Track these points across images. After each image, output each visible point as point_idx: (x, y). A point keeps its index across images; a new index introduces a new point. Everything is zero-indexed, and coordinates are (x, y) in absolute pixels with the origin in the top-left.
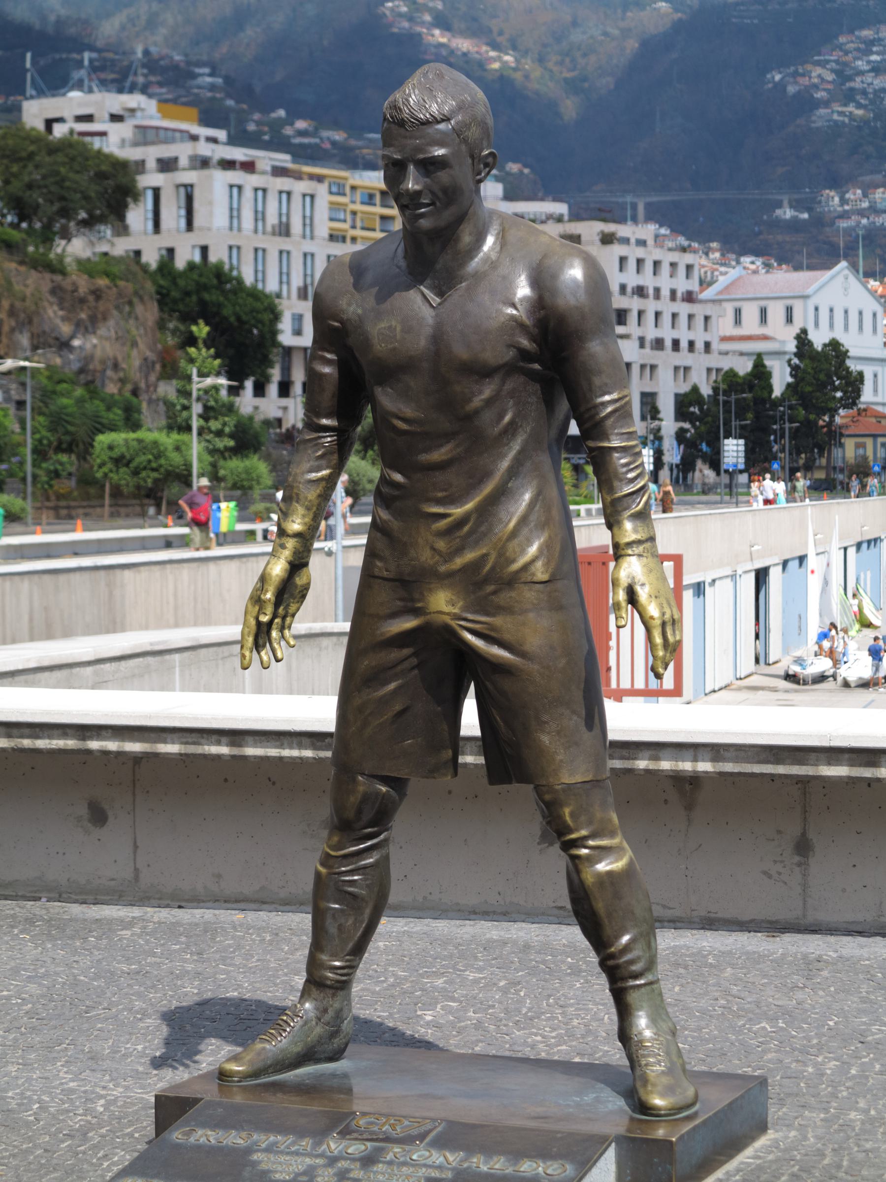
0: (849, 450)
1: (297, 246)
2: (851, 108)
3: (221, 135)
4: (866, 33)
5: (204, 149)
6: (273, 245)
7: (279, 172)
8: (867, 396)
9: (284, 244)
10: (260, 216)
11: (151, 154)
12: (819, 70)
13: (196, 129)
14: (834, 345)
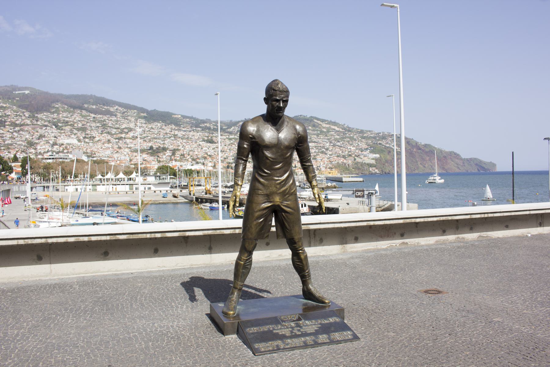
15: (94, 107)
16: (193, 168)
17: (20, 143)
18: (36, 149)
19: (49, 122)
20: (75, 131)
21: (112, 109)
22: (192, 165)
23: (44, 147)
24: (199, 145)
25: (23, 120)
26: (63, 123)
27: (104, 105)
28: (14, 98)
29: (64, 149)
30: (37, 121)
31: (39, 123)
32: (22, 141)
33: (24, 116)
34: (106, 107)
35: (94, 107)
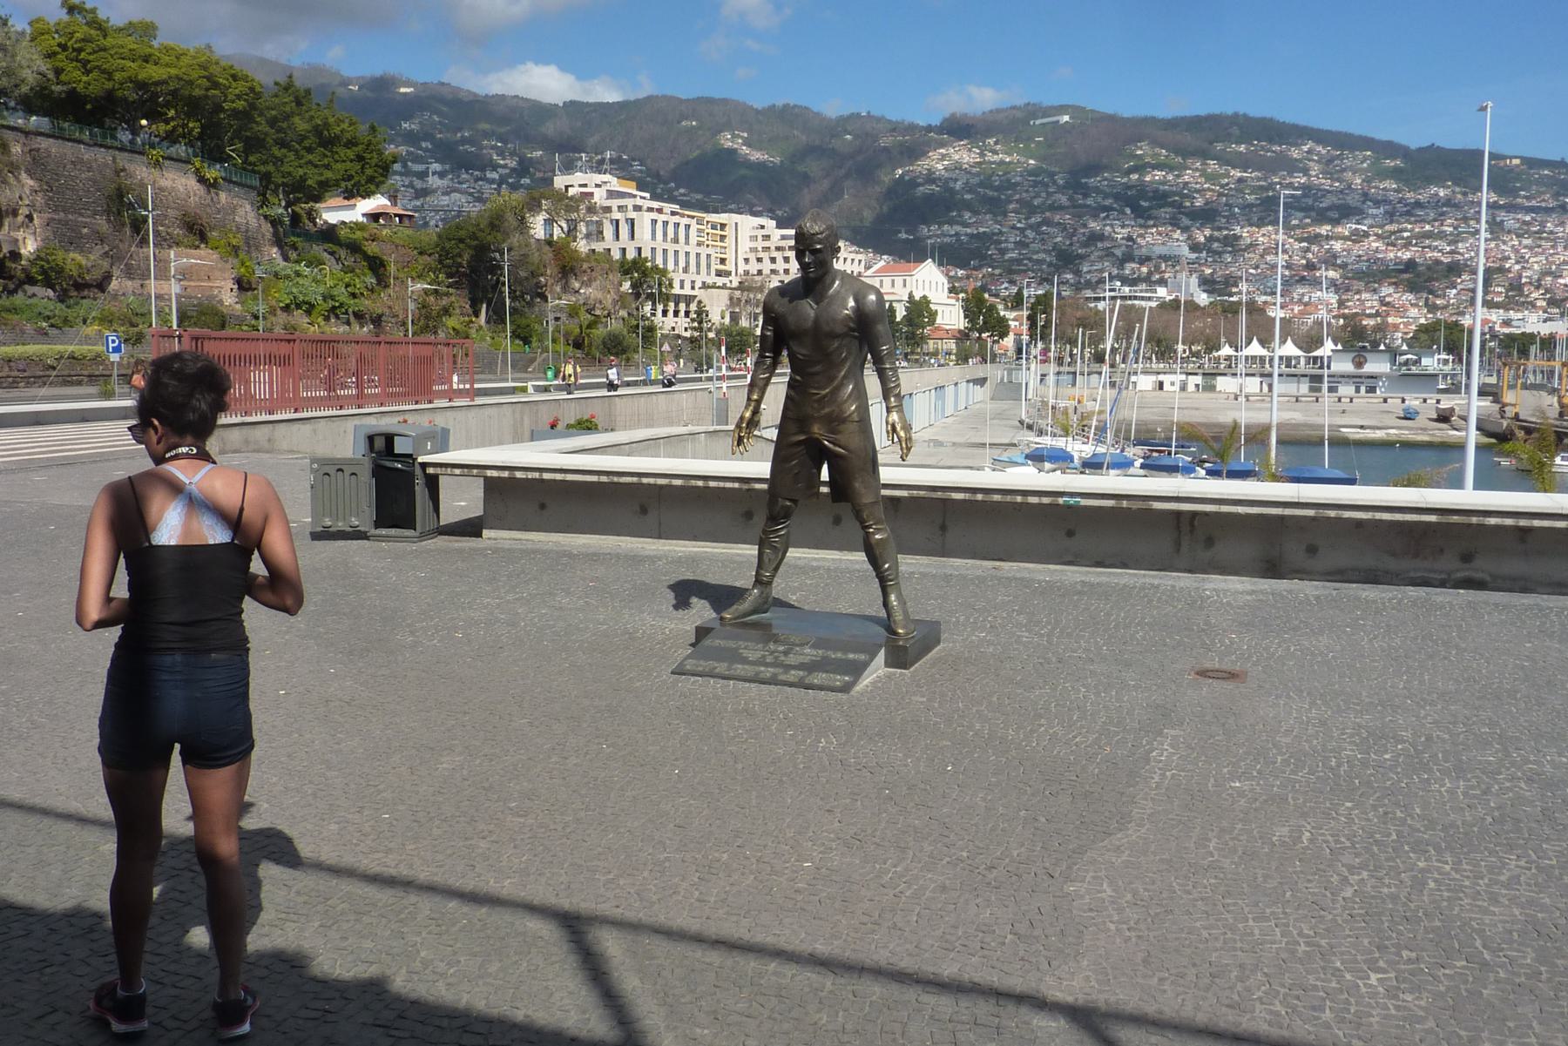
0: (931, 345)
1: (682, 248)
3: (647, 195)
4: (942, 151)
5: (639, 202)
6: (671, 248)
7: (673, 213)
8: (939, 320)
9: (676, 247)
10: (665, 234)
11: (614, 203)
13: (635, 192)
14: (925, 297)
15: (1242, 148)
17: (1041, 256)
18: (1078, 273)
19: (1117, 197)
20: (1185, 221)
21: (1295, 153)
23: (1098, 266)
25: (1049, 194)
26: (1154, 198)
27: (1271, 141)
28: (1030, 139)
29: (1150, 273)
30: (1086, 196)
31: (1089, 201)
32: (1045, 251)
33: (1055, 182)
34: (1276, 148)
35: (1242, 148)
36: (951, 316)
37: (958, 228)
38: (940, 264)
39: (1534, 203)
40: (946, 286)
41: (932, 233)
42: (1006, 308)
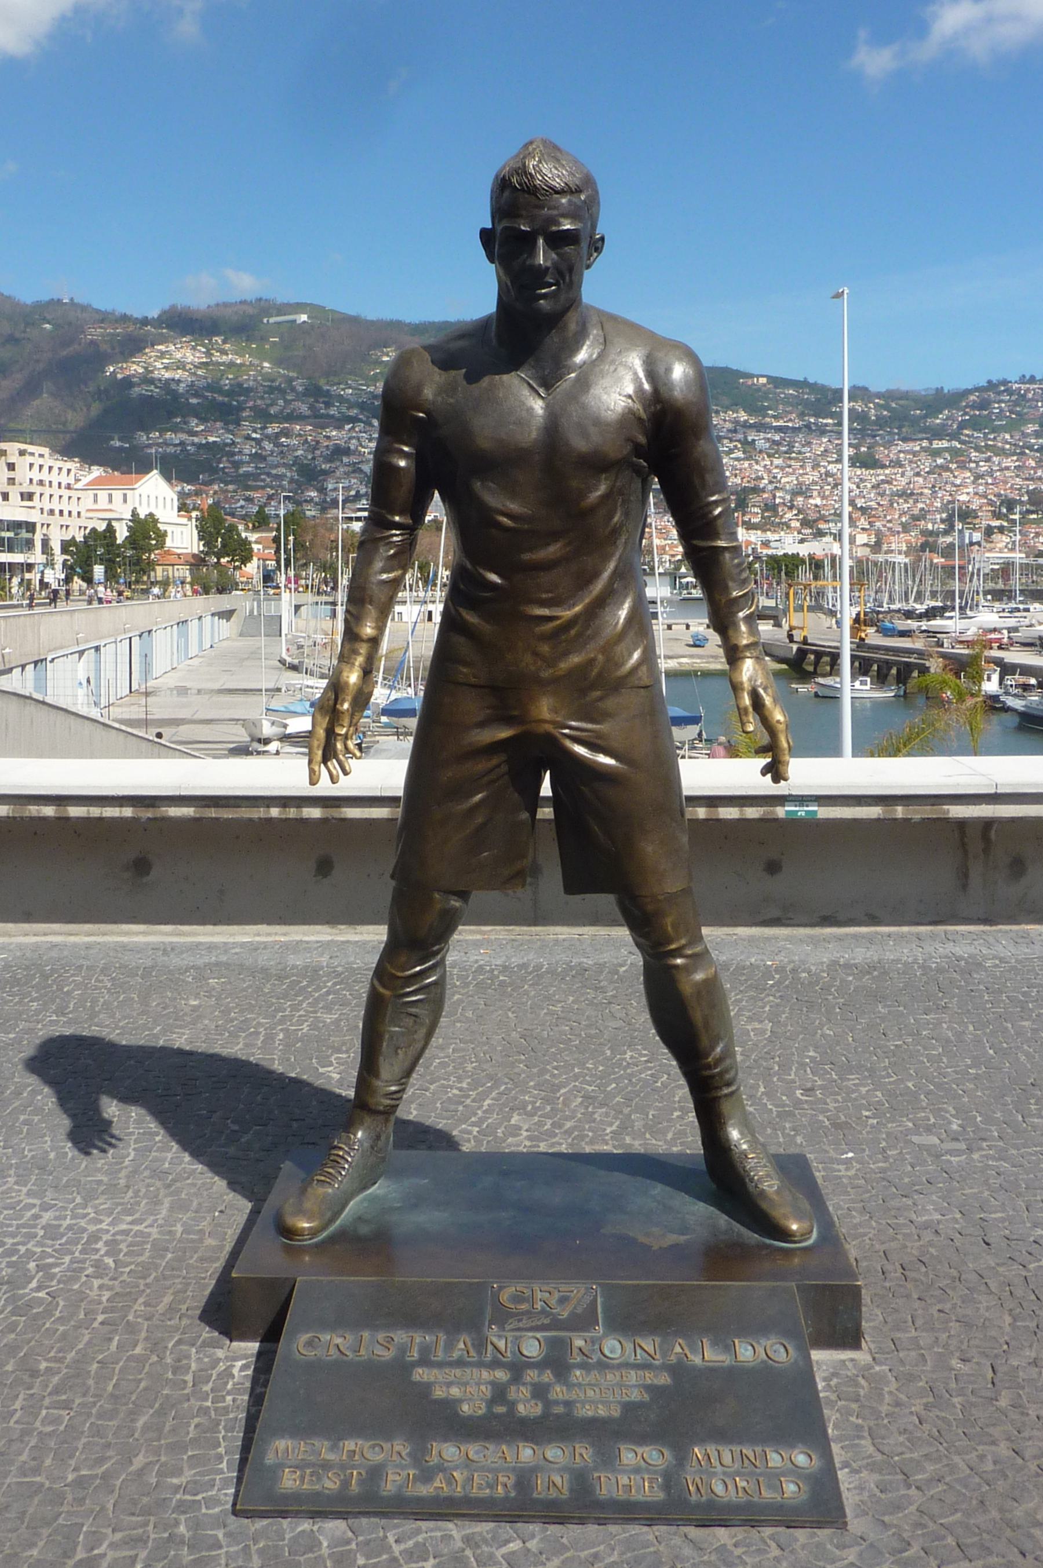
0: (159, 573)
2: (152, 387)
8: (169, 543)
12: (135, 367)
14: (151, 515)
16: (803, 551)
17: (281, 470)
18: (322, 490)
22: (802, 541)
24: (828, 474)
28: (264, 339)
30: (328, 405)
31: (333, 411)
32: (284, 465)
33: (293, 389)
36: (183, 537)
37: (183, 436)
38: (168, 478)
39: (781, 423)
40: (176, 504)
41: (153, 440)
42: (247, 529)
